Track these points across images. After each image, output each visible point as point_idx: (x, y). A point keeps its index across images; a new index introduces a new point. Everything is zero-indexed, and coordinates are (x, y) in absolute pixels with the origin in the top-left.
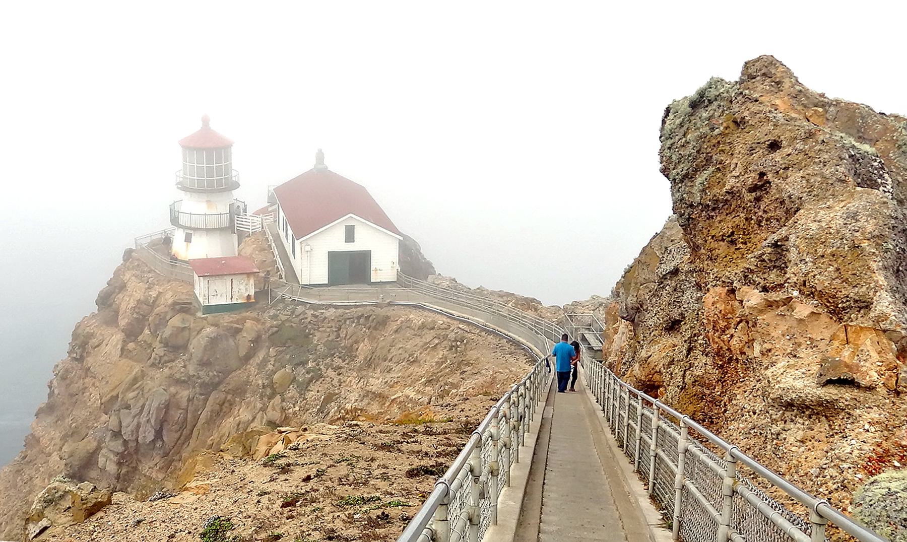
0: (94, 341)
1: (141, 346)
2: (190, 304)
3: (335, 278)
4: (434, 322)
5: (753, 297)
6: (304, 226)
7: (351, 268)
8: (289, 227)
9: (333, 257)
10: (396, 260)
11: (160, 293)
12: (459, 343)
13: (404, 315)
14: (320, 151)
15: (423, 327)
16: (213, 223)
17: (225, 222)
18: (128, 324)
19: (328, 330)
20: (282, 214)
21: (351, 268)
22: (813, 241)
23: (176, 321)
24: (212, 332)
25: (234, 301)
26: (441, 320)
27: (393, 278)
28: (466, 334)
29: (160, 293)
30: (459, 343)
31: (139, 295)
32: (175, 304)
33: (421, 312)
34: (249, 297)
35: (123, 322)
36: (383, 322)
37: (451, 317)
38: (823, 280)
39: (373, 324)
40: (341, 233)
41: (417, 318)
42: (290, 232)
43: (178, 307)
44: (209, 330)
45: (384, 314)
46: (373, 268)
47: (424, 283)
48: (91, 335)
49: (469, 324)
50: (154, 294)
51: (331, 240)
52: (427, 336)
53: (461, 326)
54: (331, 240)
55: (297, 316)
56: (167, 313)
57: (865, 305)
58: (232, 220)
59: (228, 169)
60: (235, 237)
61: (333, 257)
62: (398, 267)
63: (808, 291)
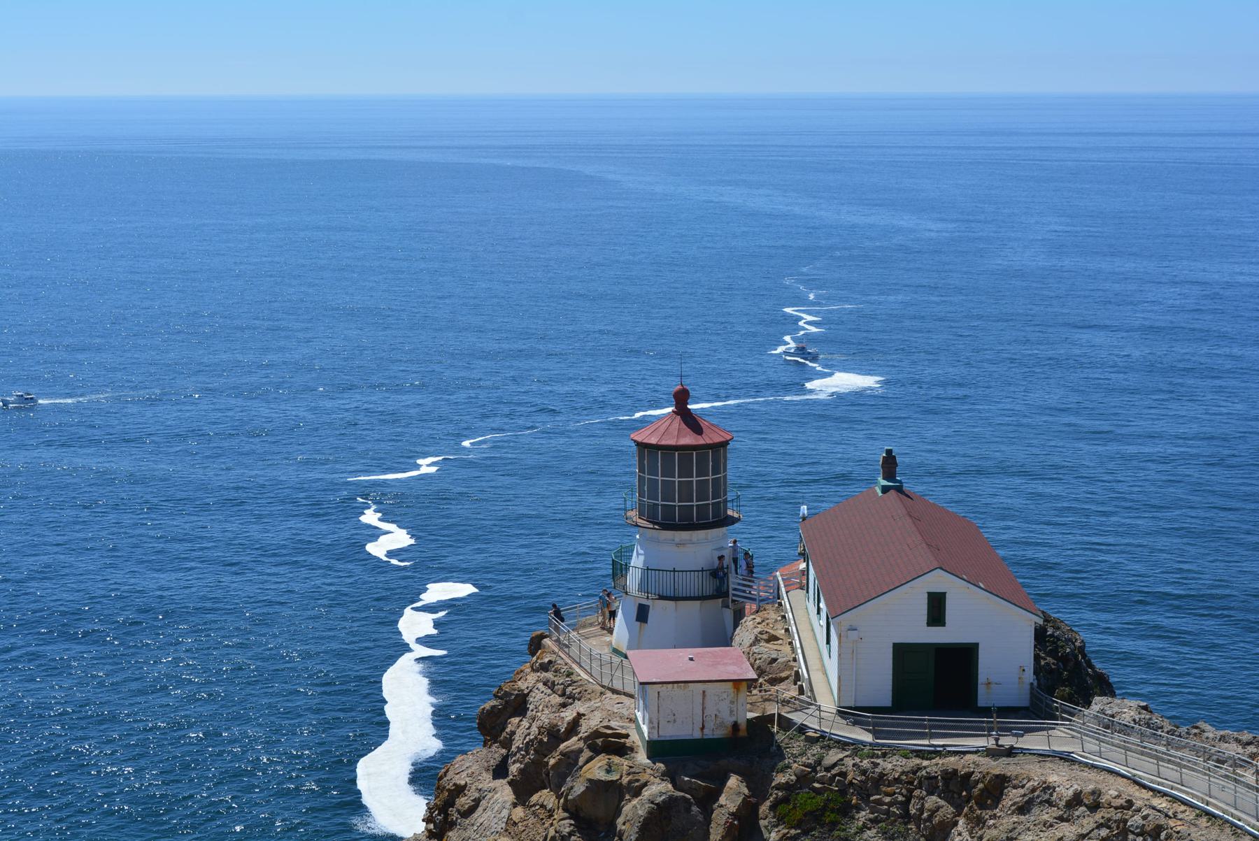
0: (463, 802)
1: (534, 813)
2: (627, 736)
4: (1096, 793)
9: (902, 652)
11: (580, 716)
13: (1037, 773)
14: (889, 452)
15: (1076, 800)
17: (709, 587)
18: (521, 771)
19: (887, 799)
23: (596, 769)
24: (661, 794)
25: (708, 734)
26: (1112, 790)
29: (580, 716)
31: (545, 718)
32: (596, 734)
34: (735, 726)
35: (514, 768)
36: (997, 787)
39: (976, 791)
40: (921, 609)
41: (1064, 782)
43: (599, 741)
44: (658, 789)
45: (997, 772)
47: (1086, 712)
48: (460, 790)
49: (1175, 799)
50: (569, 714)
52: (1085, 821)
53: (1156, 802)
55: (828, 769)
56: (581, 751)
59: (719, 487)
60: (728, 615)
61: (902, 652)
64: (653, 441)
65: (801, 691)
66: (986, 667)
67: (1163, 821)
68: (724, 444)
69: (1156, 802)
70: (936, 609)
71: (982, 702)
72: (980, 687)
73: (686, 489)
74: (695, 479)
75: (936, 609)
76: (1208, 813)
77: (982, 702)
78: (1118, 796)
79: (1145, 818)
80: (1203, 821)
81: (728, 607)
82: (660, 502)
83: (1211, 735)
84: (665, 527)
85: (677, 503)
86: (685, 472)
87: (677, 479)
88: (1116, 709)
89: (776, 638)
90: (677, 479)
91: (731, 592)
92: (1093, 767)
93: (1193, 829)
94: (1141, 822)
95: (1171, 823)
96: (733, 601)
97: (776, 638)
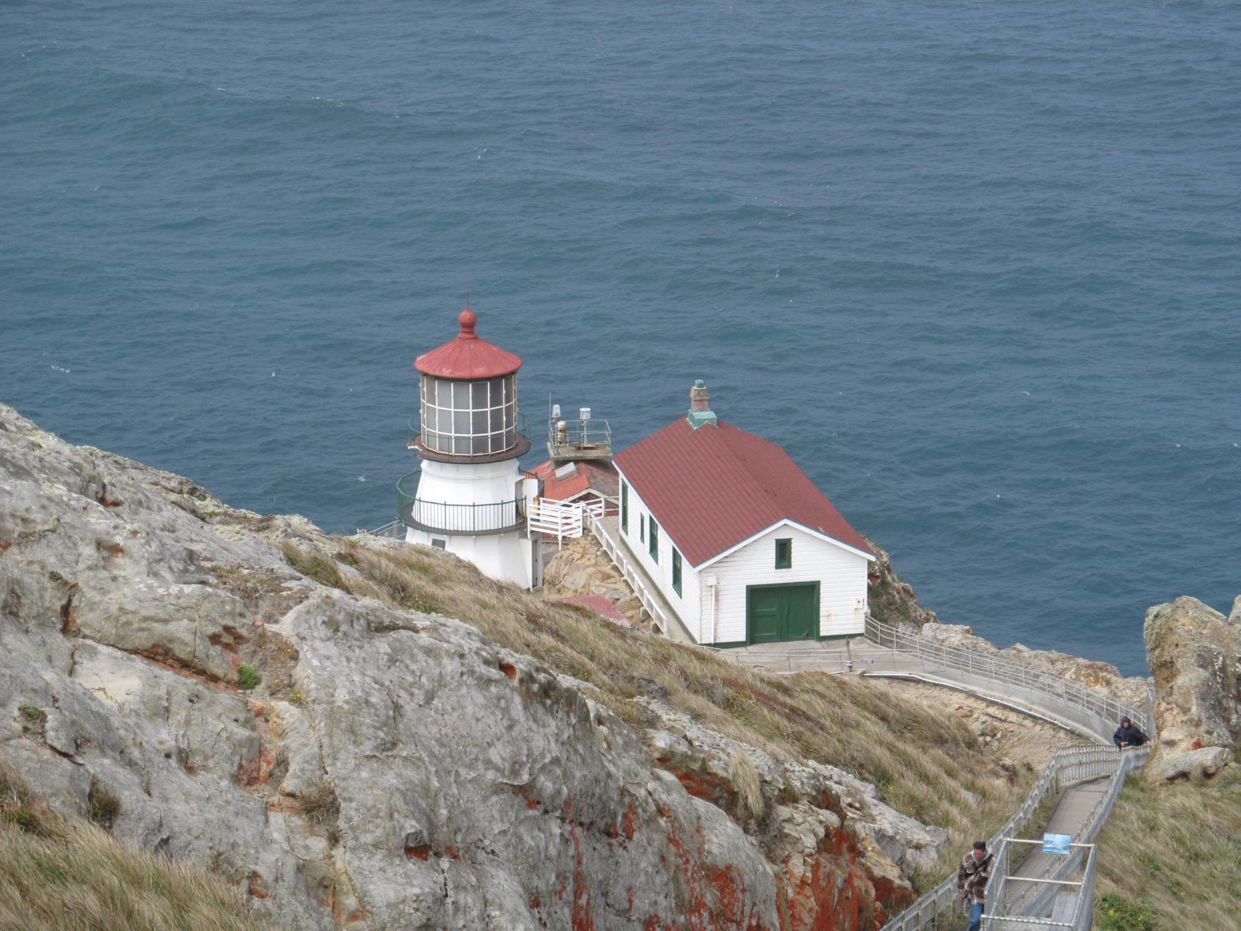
3: (757, 632)
5: (1163, 706)
6: (701, 541)
7: (783, 611)
8: (662, 535)
10: (863, 594)
12: (988, 739)
16: (489, 521)
17: (511, 520)
20: (637, 507)
21: (783, 611)
22: (1180, 688)
27: (862, 631)
28: (997, 724)
30: (988, 739)
33: (922, 690)
37: (971, 695)
38: (1180, 701)
42: (666, 543)
49: (1005, 707)
51: (754, 563)
53: (991, 710)
54: (754, 563)
57: (1189, 710)
58: (520, 514)
60: (527, 544)
62: (866, 609)
63: (1178, 706)
65: (657, 630)
67: (997, 724)
68: (513, 373)
69: (991, 710)
70: (783, 553)
71: (822, 634)
72: (821, 619)
75: (783, 553)
76: (1030, 716)
77: (822, 634)
78: (961, 707)
79: (984, 723)
80: (1028, 723)
81: (525, 536)
82: (453, 435)
83: (1026, 655)
85: (471, 435)
87: (471, 411)
88: (945, 635)
89: (609, 577)
91: (529, 522)
92: (936, 685)
93: (1022, 729)
94: (981, 727)
95: (1006, 725)
96: (532, 532)
97: (609, 577)
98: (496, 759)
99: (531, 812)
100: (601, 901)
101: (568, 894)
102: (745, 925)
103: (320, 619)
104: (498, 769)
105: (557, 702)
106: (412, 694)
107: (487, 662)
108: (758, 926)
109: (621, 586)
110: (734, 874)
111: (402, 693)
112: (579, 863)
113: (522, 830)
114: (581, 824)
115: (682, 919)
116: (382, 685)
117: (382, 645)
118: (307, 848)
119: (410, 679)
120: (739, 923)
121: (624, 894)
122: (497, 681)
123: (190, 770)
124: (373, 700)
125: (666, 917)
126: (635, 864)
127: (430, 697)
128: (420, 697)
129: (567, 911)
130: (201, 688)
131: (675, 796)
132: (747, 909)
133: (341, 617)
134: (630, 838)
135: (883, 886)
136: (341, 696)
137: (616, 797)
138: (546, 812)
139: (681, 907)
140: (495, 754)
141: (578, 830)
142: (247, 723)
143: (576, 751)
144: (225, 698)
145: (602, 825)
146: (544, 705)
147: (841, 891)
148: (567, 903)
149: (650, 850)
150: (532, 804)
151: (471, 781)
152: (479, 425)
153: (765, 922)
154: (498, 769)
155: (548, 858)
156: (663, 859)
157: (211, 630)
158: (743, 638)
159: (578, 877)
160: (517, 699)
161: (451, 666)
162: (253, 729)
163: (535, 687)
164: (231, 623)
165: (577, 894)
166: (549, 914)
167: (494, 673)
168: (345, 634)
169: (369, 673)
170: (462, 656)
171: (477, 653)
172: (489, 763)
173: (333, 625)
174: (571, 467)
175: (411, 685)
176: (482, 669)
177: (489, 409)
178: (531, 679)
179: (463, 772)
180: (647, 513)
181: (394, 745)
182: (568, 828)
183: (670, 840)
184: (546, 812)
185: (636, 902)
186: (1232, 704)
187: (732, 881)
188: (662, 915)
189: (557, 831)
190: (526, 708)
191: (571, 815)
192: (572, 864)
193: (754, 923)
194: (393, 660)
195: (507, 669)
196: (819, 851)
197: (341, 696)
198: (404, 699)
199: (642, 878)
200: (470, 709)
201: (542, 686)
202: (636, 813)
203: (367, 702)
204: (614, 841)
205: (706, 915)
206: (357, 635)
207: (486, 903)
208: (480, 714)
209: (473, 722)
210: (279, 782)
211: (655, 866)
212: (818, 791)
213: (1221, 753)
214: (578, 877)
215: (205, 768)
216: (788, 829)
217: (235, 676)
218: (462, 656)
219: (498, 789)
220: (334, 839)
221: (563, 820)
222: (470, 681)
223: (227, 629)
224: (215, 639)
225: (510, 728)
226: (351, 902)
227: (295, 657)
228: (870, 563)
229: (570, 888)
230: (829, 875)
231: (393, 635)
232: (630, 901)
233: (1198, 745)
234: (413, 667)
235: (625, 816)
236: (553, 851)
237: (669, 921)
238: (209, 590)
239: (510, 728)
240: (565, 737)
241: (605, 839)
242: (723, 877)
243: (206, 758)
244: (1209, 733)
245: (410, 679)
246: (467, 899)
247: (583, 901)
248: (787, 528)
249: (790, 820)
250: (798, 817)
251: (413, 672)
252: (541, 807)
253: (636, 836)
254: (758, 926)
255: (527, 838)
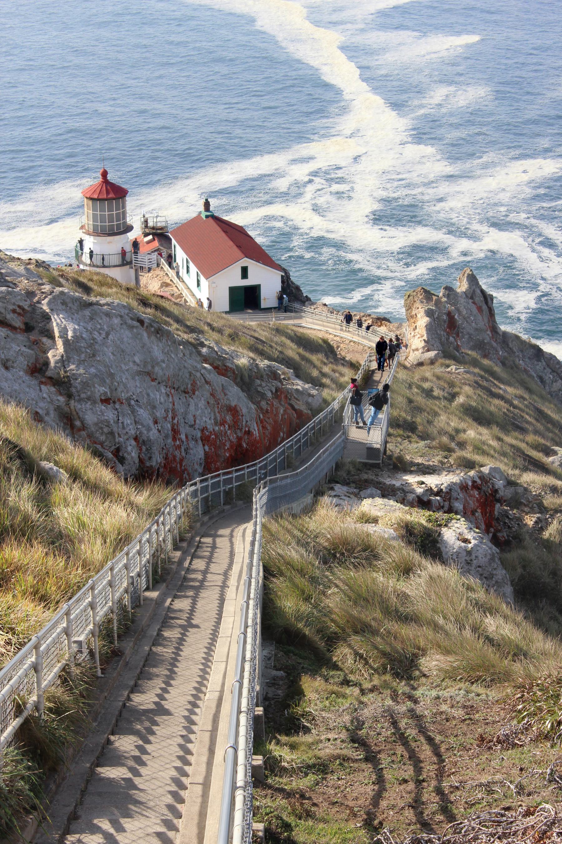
9: (233, 291)
42: (193, 269)
46: (262, 297)
51: (232, 278)
61: (233, 291)
64: (96, 196)
66: (264, 293)
70: (245, 272)
71: (262, 307)
73: (110, 216)
74: (114, 213)
75: (245, 272)
77: (262, 307)
81: (132, 268)
82: (99, 224)
84: (110, 235)
85: (107, 224)
86: (110, 210)
87: (107, 213)
90: (107, 213)
91: (134, 262)
98: (137, 361)
99: (153, 383)
100: (182, 420)
101: (170, 418)
102: (243, 431)
103: (59, 301)
104: (138, 365)
105: (162, 336)
106: (100, 334)
107: (132, 319)
108: (249, 431)
109: (175, 289)
110: (239, 409)
111: (96, 333)
112: (174, 405)
113: (149, 391)
114: (174, 388)
115: (217, 428)
116: (87, 329)
117: (87, 312)
118: (58, 400)
119: (99, 327)
120: (241, 430)
121: (192, 418)
122: (136, 327)
123: (7, 368)
124: (84, 336)
125: (210, 428)
126: (196, 405)
127: (108, 334)
128: (104, 335)
129: (169, 425)
130: (9, 332)
131: (212, 375)
132: (244, 423)
133: (68, 301)
134: (194, 394)
135: (300, 414)
136: (70, 334)
137: (188, 376)
138: (159, 383)
139: (216, 423)
140: (137, 359)
141: (173, 391)
142: (29, 348)
143: (171, 357)
144: (21, 337)
145: (182, 388)
146: (156, 337)
147: (282, 415)
148: (169, 422)
149: (203, 399)
150: (153, 380)
151: (127, 370)
152: (111, 220)
153: (251, 429)
154: (138, 365)
155: (161, 403)
156: (208, 403)
157: (11, 307)
158: (228, 310)
159: (173, 410)
160: (145, 334)
161: (116, 321)
162: (32, 350)
163: (153, 329)
164: (21, 304)
165: (173, 418)
166: (161, 427)
167: (136, 323)
168: (70, 308)
169: (81, 324)
170: (121, 316)
171: (127, 315)
172: (134, 362)
173: (64, 303)
174: (150, 237)
175: (100, 329)
176: (130, 322)
177: (114, 213)
178: (152, 326)
179: (123, 366)
180: (185, 256)
181: (94, 355)
182: (168, 389)
183: (211, 394)
184: (159, 383)
185: (197, 421)
186: (442, 333)
187: (237, 411)
188: (209, 427)
189: (163, 391)
190: (149, 337)
191: (170, 383)
192: (171, 406)
193: (247, 429)
194: (91, 319)
195: (141, 322)
196: (273, 398)
197: (70, 334)
198: (96, 335)
199: (200, 411)
200: (125, 339)
201: (155, 329)
202: (196, 383)
203: (82, 337)
204: (187, 395)
205: (227, 426)
206: (75, 308)
207: (136, 422)
208: (130, 341)
209: (127, 345)
210: (45, 373)
211: (205, 406)
212: (271, 372)
213: (438, 353)
214: (173, 410)
215: (13, 367)
216: (259, 389)
217: (22, 327)
218: (121, 316)
219: (139, 373)
220: (70, 396)
221: (166, 387)
222: (125, 327)
223: (19, 306)
224: (14, 311)
225: (143, 347)
226: (78, 423)
227: (49, 319)
228: (282, 276)
229: (170, 415)
230: (277, 409)
231: (91, 308)
232: (195, 421)
233: (428, 350)
234: (100, 321)
235: (192, 385)
236: (162, 400)
237: (212, 429)
238: (10, 289)
239: (143, 347)
240: (166, 350)
241: (184, 395)
242: (234, 411)
243: (13, 362)
244: (433, 345)
245: (99, 327)
246: (128, 421)
247: (175, 421)
248: (246, 262)
249: (260, 385)
250: (264, 384)
251: (100, 324)
252: (157, 381)
253: (197, 393)
254: (249, 431)
255: (151, 395)
